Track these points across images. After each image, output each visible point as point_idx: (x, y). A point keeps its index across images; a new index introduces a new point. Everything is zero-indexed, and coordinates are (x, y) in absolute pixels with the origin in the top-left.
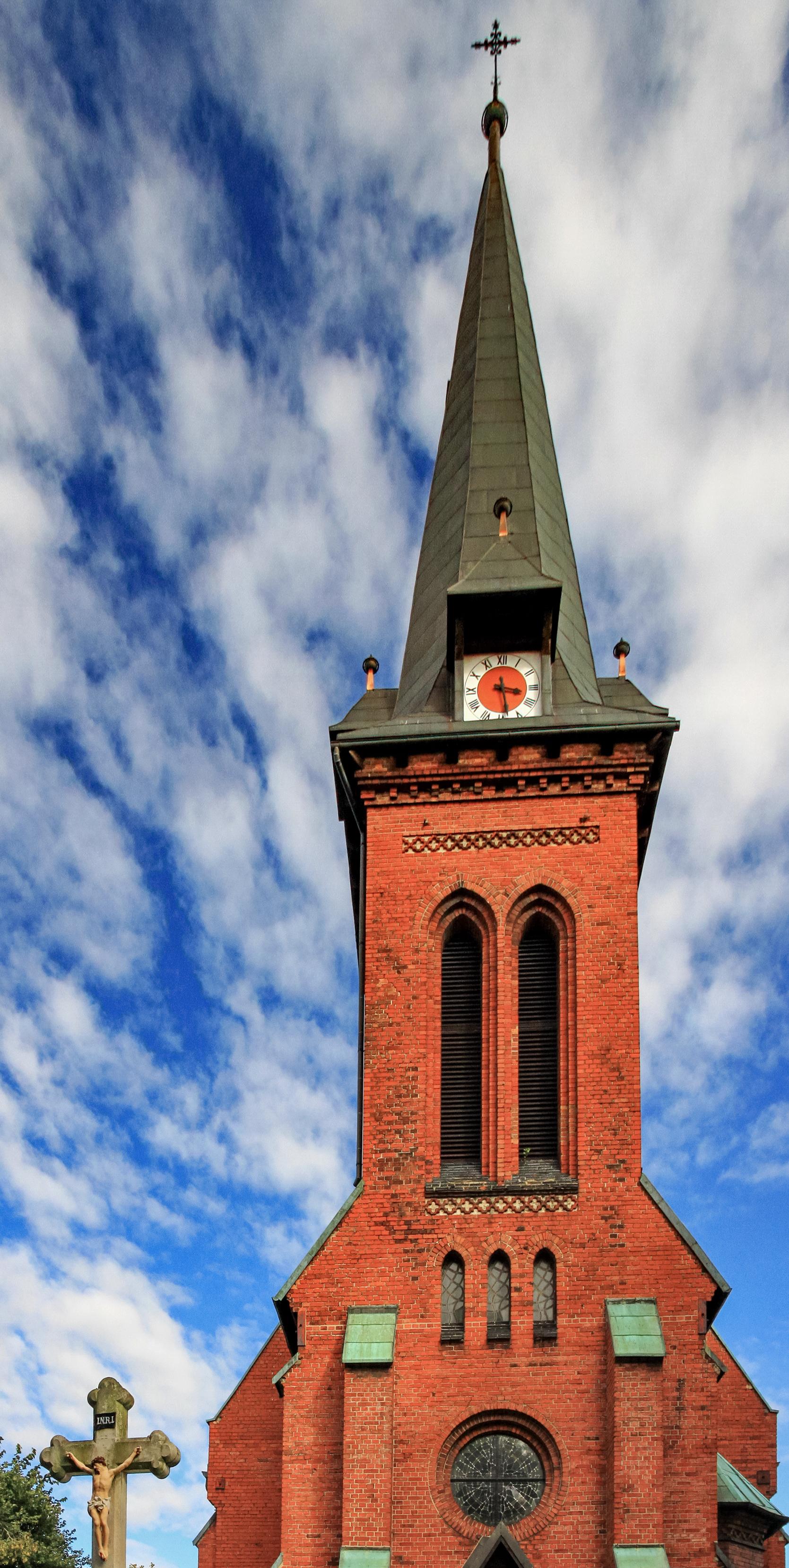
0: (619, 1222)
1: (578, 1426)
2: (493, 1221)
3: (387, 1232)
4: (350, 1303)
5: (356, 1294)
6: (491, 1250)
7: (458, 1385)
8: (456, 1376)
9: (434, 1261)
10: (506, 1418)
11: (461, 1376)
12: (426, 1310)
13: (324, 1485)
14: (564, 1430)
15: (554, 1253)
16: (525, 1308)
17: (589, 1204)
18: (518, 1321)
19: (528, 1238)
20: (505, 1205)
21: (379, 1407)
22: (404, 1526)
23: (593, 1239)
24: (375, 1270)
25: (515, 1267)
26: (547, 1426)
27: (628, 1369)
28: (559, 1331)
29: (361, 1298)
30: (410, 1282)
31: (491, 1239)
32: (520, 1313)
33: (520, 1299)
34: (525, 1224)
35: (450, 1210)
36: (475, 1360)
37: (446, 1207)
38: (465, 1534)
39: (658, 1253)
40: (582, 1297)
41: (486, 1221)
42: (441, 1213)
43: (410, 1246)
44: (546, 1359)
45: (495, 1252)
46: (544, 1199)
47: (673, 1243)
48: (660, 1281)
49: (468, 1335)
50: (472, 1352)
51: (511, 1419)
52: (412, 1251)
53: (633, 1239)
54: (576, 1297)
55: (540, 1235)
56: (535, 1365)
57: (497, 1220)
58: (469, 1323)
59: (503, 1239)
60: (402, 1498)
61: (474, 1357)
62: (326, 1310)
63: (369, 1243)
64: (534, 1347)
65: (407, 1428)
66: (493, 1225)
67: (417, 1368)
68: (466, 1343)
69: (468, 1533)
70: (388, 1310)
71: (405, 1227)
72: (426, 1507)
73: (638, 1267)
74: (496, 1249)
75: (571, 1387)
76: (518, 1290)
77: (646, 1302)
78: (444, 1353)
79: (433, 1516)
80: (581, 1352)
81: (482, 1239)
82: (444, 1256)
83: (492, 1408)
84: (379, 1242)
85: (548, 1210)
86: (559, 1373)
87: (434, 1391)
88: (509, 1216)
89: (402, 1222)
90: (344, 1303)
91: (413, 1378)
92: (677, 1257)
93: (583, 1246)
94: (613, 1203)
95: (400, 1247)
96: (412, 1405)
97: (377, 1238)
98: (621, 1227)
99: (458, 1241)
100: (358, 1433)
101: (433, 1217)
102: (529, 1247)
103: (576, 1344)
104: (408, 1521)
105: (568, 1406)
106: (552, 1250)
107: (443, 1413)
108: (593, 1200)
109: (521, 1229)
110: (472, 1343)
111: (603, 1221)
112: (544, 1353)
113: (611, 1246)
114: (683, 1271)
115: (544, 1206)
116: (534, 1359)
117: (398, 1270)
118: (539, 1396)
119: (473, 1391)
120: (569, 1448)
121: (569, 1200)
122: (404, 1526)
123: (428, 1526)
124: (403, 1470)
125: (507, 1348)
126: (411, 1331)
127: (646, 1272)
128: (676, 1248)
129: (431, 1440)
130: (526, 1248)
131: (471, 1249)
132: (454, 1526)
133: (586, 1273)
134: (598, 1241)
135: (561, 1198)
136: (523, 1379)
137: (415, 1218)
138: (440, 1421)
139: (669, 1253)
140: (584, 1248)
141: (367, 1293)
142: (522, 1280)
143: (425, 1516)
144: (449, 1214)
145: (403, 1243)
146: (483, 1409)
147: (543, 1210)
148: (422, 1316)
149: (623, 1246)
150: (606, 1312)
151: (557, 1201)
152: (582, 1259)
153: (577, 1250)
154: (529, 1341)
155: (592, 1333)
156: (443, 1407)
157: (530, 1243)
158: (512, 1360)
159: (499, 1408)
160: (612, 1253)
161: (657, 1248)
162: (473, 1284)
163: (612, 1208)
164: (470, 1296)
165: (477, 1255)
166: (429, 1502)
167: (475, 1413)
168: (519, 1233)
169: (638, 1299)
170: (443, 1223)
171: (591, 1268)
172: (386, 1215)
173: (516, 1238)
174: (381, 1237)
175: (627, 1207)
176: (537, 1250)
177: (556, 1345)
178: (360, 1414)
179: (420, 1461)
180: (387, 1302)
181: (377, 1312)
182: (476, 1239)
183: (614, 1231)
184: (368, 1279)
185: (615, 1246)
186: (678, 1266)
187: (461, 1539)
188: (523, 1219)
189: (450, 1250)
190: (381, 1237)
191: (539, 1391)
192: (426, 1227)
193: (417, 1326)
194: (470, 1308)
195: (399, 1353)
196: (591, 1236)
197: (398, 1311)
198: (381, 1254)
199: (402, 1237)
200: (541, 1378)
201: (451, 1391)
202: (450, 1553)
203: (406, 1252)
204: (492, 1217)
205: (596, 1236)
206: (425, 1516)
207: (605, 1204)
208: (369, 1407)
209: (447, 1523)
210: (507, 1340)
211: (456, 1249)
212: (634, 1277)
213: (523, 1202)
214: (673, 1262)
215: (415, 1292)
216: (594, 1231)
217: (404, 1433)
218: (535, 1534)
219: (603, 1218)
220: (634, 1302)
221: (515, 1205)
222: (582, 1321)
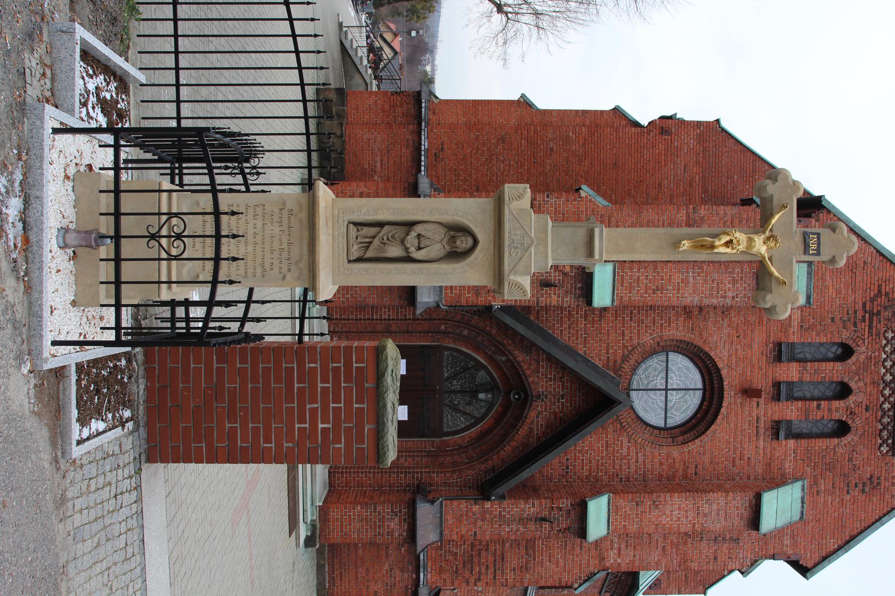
0: (867, 490)
1: (706, 458)
2: (876, 385)
5: (824, 269)
6: (853, 385)
8: (752, 356)
9: (845, 336)
11: (752, 360)
12: (807, 330)
14: (704, 447)
17: (883, 465)
20: (888, 395)
22: (631, 312)
23: (855, 468)
24: (842, 286)
25: (836, 404)
26: (708, 432)
27: (750, 502)
29: (820, 274)
30: (830, 315)
33: (811, 408)
34: (871, 411)
35: (887, 349)
37: (889, 346)
38: (623, 365)
39: (840, 521)
41: (876, 380)
42: (884, 342)
43: (859, 315)
44: (762, 431)
46: (890, 428)
49: (784, 365)
51: (715, 402)
52: (855, 318)
53: (852, 501)
55: (861, 425)
56: (757, 422)
57: (875, 388)
58: (794, 366)
59: (860, 394)
60: (654, 310)
66: (872, 386)
68: (778, 364)
69: (624, 368)
71: (875, 311)
72: (646, 332)
73: (830, 505)
74: (853, 388)
75: (738, 452)
78: (771, 345)
79: (639, 339)
81: (861, 376)
85: (881, 431)
86: (749, 442)
87: (741, 337)
88: (878, 399)
89: (879, 308)
94: (882, 484)
95: (859, 306)
96: (730, 318)
98: (863, 491)
101: (882, 335)
104: (635, 316)
105: (723, 449)
107: (722, 345)
108: (887, 468)
109: (867, 409)
111: (868, 477)
112: (766, 429)
113: (848, 483)
115: (884, 428)
116: (762, 421)
117: (840, 306)
118: (732, 426)
120: (689, 451)
121: (888, 448)
122: (631, 312)
123: (631, 333)
124: (677, 312)
125: (773, 398)
128: (843, 535)
129: (701, 335)
130: (851, 413)
131: (854, 367)
132: (630, 356)
134: (853, 472)
135: (890, 441)
136: (747, 412)
137: (882, 320)
138: (716, 343)
139: (840, 530)
142: (826, 410)
143: (639, 331)
144: (884, 348)
147: (881, 427)
148: (802, 326)
149: (848, 492)
150: (797, 480)
151: (888, 439)
154: (776, 417)
156: (727, 345)
157: (855, 416)
160: (842, 484)
161: (844, 520)
163: (878, 484)
164: (816, 367)
166: (651, 334)
167: (722, 373)
168: (864, 407)
169: (805, 505)
170: (876, 343)
171: (831, 467)
172: (887, 294)
175: (879, 497)
176: (850, 422)
179: (684, 326)
180: (815, 296)
181: (807, 287)
182: (861, 371)
183: (860, 486)
185: (848, 487)
186: (828, 537)
187: (619, 362)
188: (875, 410)
189: (854, 349)
191: (736, 426)
192: (874, 329)
193: (794, 322)
199: (868, 309)
200: (746, 427)
201: (740, 352)
202: (608, 353)
203: (855, 312)
204: (878, 385)
206: (639, 331)
207: (883, 478)
209: (633, 349)
210: (779, 400)
211: (855, 355)
213: (889, 409)
215: (822, 319)
216: (861, 469)
218: (621, 424)
219: (871, 476)
220: (803, 502)
221: (887, 403)
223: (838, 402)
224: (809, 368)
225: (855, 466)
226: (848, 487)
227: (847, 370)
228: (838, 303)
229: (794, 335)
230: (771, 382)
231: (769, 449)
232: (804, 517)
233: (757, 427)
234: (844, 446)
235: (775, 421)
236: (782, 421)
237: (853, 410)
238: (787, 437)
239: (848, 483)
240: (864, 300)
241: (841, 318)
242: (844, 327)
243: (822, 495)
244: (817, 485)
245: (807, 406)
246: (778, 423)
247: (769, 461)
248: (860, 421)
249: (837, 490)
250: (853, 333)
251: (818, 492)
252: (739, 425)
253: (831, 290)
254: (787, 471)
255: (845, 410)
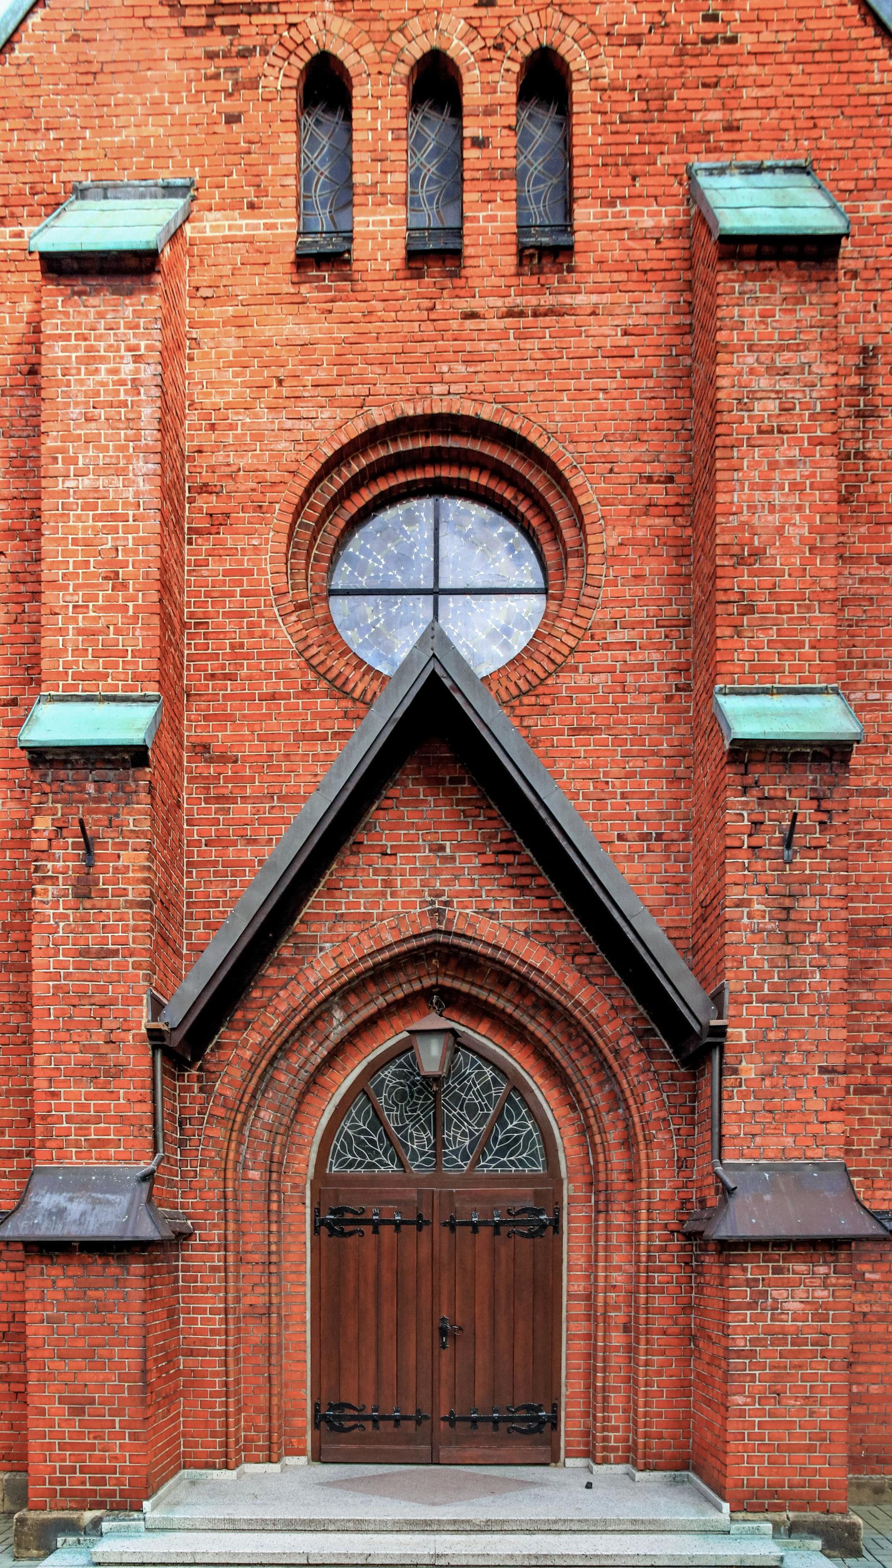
3: (166, 11)
4: (80, 176)
5: (91, 154)
6: (416, 50)
7: (340, 360)
10: (452, 443)
13: (23, 588)
15: (568, 58)
16: (496, 185)
18: (481, 215)
19: (504, 22)
21: (127, 368)
24: (138, 100)
28: (578, 237)
29: (106, 163)
30: (222, 128)
31: (415, 25)
32: (486, 197)
33: (485, 164)
36: (380, 305)
39: (818, 57)
40: (634, 160)
43: (220, 43)
45: (425, 56)
47: (855, 33)
48: (822, 123)
49: (360, 250)
50: (370, 286)
53: (758, 26)
54: (620, 160)
55: (534, 17)
56: (521, 314)
61: (374, 298)
62: (21, 194)
63: (120, 35)
64: (518, 274)
65: (219, 458)
67: (239, 322)
68: (356, 266)
70: (170, 190)
73: (768, 91)
74: (427, 48)
76: (479, 143)
77: (787, 169)
78: (304, 289)
80: (631, 286)
81: (394, 26)
82: (301, 65)
83: (419, 411)
84: (144, 33)
87: (281, 373)
90: (64, 176)
91: (231, 344)
92: (865, 66)
93: (636, 40)
95: (196, 46)
97: (139, 23)
99: (334, 30)
100: (78, 427)
102: (507, 45)
103: (619, 267)
106: (562, 51)
110: (370, 265)
113: (705, 41)
114: (877, 99)
116: (519, 300)
118: (531, 385)
119: (373, 372)
126: (227, 240)
127: (788, 102)
128: (861, 45)
130: (499, 47)
131: (368, 50)
133: (643, 106)
134: (673, 28)
136: (494, 346)
139: (843, 56)
140: (639, 45)
141: (120, 153)
142: (490, 120)
145: (203, 35)
146: (398, 414)
148: (252, 206)
152: (634, 73)
153: (621, 52)
154: (509, 262)
155: (658, 241)
157: (507, 34)
158: (464, 304)
159: (436, 411)
160: (707, 60)
161: (816, 46)
162: (374, 130)
164: (367, 157)
165: (382, 62)
167: (380, 422)
168: (482, 12)
169: (767, 163)
171: (655, 94)
173: (475, 23)
174: (150, 23)
176: (526, 51)
177: (570, 270)
178: (81, 382)
181: (142, 196)
182: (378, 26)
184: (122, 121)
186: (864, 88)
189: (315, 51)
190: (150, 23)
193: (240, 228)
194: (364, 185)
195: (197, 289)
196: (657, 18)
197: (192, 193)
198: (154, 62)
199: (202, 21)
203: (211, 56)
205: (669, 18)
208: (103, 367)
210: (456, 254)
211: (331, 48)
212: (757, 113)
214: (854, 79)
217: (212, 469)
220: (759, 170)
222: (633, 213)
223: (466, 89)
224: (369, 179)
225: (652, 26)
226: (714, 41)
227: (374, 70)
228: (185, 107)
229: (273, 226)
230: (408, 284)
231: (600, 277)
232: (801, 162)
233: (535, 315)
234: (596, 62)
235: (520, 264)
236: (519, 243)
237: (490, 42)
238: (567, 227)
239: (705, 41)
240: (178, 33)
241: (229, 95)
242: (253, 84)
243: (738, 115)
244: (708, 133)
245: (479, 175)
246: (522, 254)
247: (635, 276)
248: (524, 19)
249: (724, 72)
250: (270, 58)
251: (731, 127)
252: (530, 365)
253: (150, 130)
254: (665, 221)
255: (487, 66)
